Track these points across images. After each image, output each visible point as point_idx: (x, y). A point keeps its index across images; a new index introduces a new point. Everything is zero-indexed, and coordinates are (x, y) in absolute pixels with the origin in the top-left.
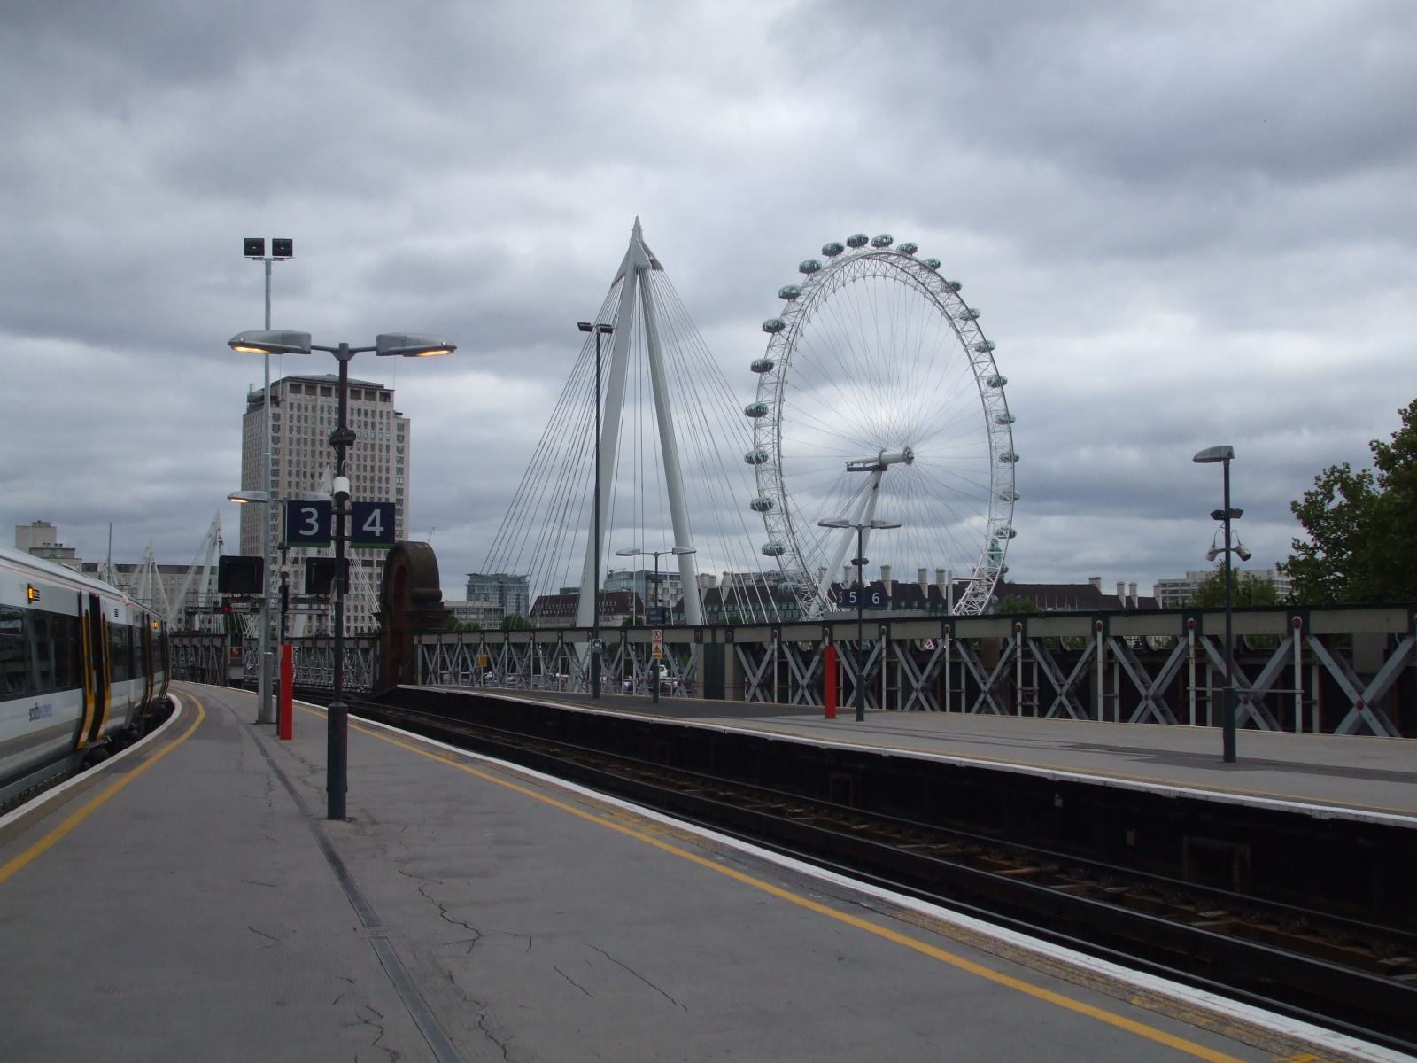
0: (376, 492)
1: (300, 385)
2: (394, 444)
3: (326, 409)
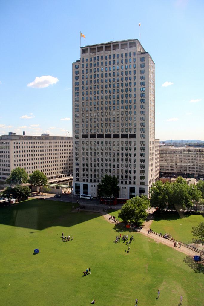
0: (128, 97)
1: (87, 49)
2: (138, 69)
3: (100, 58)
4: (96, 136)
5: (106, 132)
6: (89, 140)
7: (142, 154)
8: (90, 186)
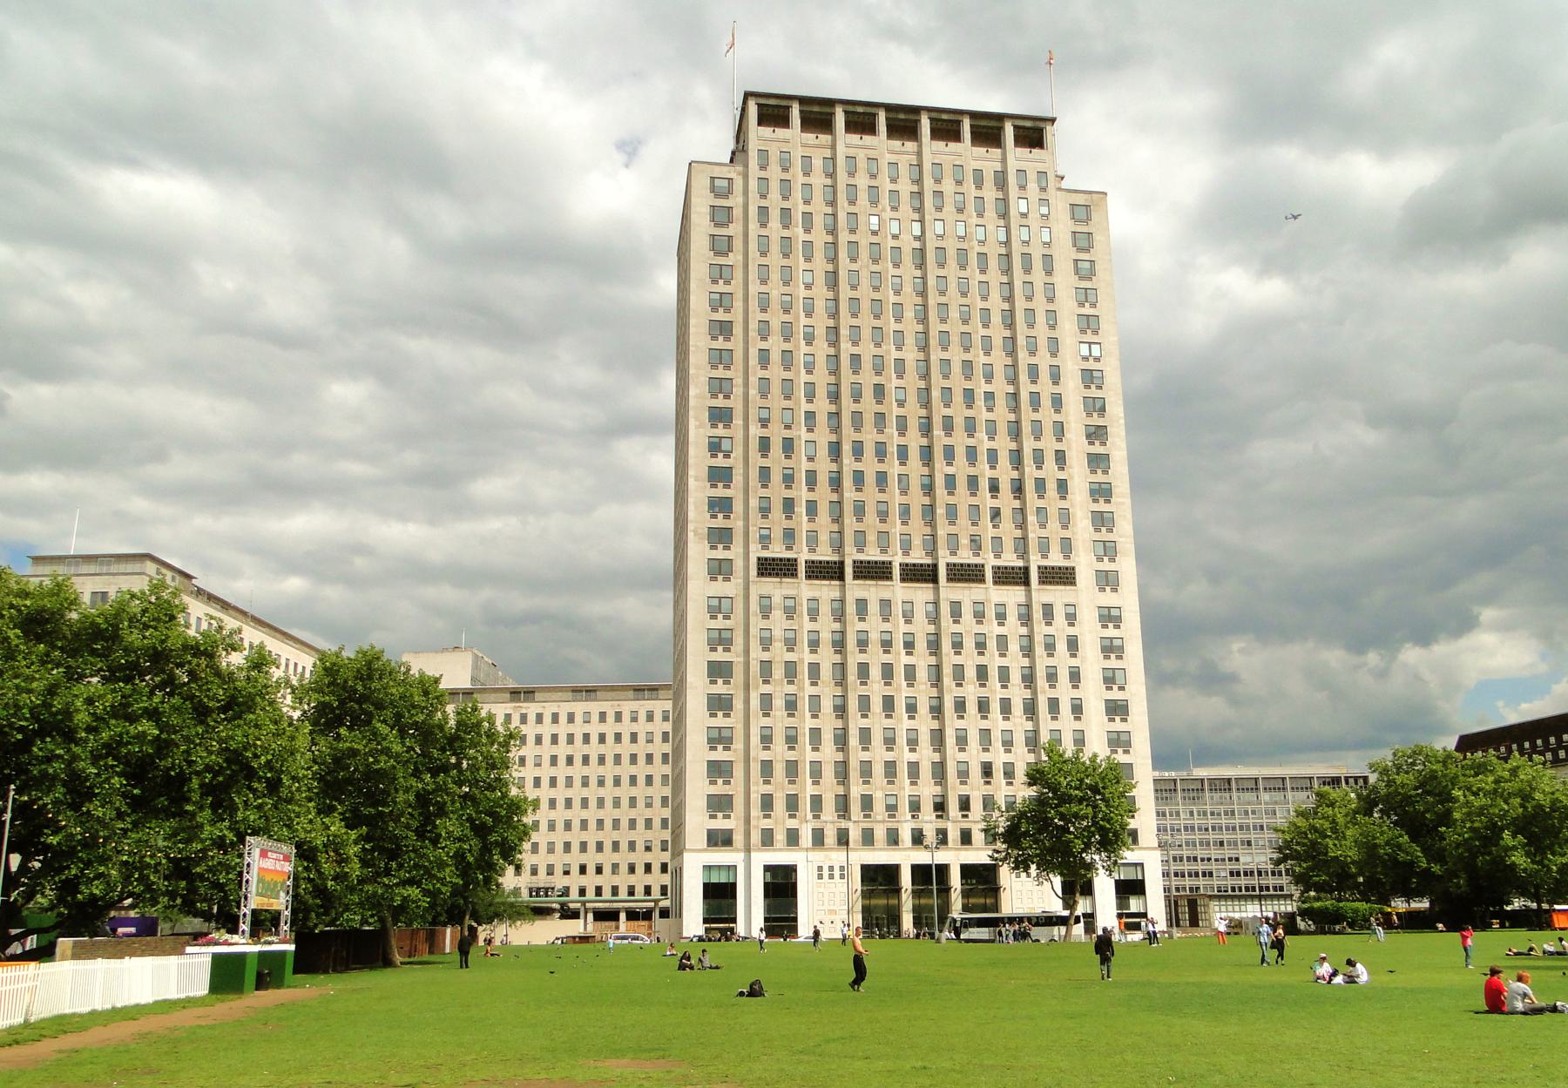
2: (1064, 255)
3: (862, 164)
4: (849, 570)
5: (906, 553)
6: (805, 589)
7: (1110, 674)
8: (816, 873)
